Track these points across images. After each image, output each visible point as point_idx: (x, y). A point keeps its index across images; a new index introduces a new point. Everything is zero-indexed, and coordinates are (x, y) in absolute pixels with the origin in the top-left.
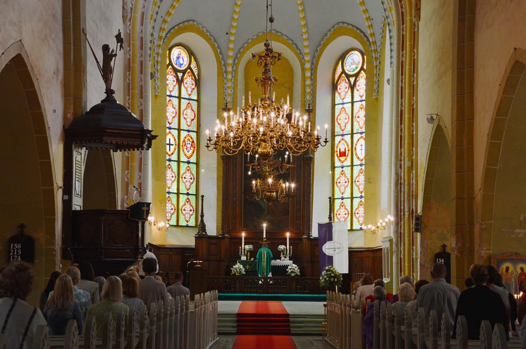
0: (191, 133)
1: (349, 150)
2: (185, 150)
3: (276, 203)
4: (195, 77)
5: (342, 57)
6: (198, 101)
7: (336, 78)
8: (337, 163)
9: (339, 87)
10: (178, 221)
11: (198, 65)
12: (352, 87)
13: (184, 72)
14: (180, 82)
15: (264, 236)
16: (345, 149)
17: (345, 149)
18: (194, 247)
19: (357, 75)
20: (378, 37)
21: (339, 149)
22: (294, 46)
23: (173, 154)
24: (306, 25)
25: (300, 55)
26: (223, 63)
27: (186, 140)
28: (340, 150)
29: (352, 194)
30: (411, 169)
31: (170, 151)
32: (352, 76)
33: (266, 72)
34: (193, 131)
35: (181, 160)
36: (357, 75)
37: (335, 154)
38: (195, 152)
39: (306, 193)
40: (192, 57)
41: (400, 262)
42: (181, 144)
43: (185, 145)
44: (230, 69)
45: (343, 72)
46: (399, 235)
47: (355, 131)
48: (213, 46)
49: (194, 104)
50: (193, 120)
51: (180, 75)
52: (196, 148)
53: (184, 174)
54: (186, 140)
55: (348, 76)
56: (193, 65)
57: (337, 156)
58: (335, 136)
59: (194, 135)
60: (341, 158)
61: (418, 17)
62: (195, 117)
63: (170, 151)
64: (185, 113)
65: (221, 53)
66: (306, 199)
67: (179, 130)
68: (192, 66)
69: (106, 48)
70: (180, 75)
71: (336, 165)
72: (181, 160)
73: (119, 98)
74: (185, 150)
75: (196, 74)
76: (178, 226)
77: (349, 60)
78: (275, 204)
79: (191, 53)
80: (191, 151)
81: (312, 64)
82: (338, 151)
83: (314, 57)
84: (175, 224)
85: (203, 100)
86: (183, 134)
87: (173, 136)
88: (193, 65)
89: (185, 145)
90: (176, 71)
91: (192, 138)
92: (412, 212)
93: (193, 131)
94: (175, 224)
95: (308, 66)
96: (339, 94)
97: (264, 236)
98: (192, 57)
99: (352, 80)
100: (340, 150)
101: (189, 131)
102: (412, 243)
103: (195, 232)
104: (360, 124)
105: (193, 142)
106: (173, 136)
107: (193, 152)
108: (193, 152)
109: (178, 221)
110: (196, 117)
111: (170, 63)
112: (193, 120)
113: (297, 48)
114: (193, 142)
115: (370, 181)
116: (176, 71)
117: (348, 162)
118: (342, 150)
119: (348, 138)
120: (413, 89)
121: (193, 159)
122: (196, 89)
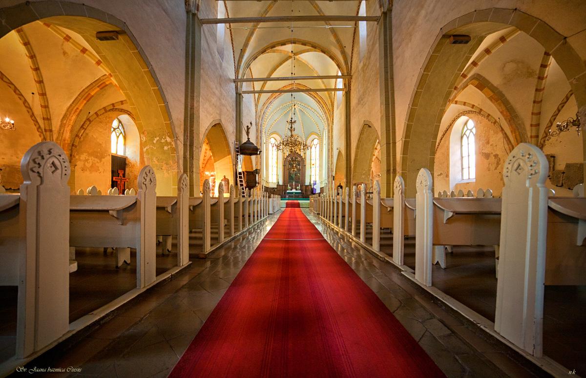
20: (321, 133)
30: (331, 164)
41: (329, 188)
46: (329, 182)
61: (333, 124)
69: (248, 126)
73: (251, 141)
92: (332, 176)
102: (332, 183)
104: (318, 157)
120: (332, 143)
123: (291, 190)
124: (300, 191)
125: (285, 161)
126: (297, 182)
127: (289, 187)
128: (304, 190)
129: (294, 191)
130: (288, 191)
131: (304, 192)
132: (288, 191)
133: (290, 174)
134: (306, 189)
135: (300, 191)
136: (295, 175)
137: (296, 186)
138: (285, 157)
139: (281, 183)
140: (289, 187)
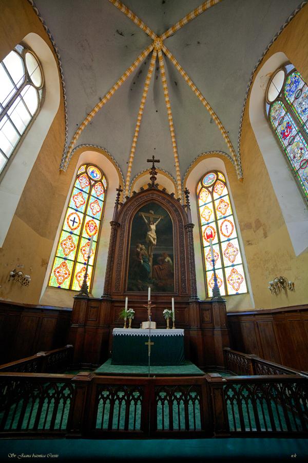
0: (94, 220)
1: (215, 232)
2: (88, 230)
3: (161, 266)
4: (104, 188)
5: (201, 180)
6: (104, 202)
7: (198, 191)
8: (205, 243)
9: (200, 196)
10: (71, 285)
11: (107, 182)
12: (212, 193)
13: (96, 182)
14: (92, 186)
15: (149, 299)
16: (212, 232)
17: (212, 232)
18: (71, 310)
19: (213, 185)
21: (206, 233)
22: (170, 175)
23: (75, 229)
24: (178, 157)
25: (174, 180)
26: (123, 180)
27: (90, 223)
28: (207, 234)
29: (223, 264)
31: (73, 226)
32: (210, 187)
33: (153, 178)
34: (97, 219)
35: (83, 236)
36: (213, 185)
37: (203, 238)
38: (97, 234)
39: (189, 257)
40: (104, 177)
42: (85, 225)
43: (89, 226)
44: (128, 183)
45: (203, 187)
47: (218, 218)
48: (118, 170)
49: (101, 204)
50: (98, 212)
51: (93, 183)
52: (98, 231)
53: (84, 247)
54: (90, 223)
55: (207, 188)
56: (104, 181)
57: (205, 239)
58: (201, 226)
59: (98, 223)
60: (209, 240)
62: (100, 210)
63: (73, 226)
64: (92, 205)
65: (123, 175)
66: (190, 262)
67: (85, 214)
68: (102, 181)
70: (93, 183)
71: (205, 246)
72: (83, 236)
74: (88, 230)
75: (105, 186)
76: (70, 290)
77: (206, 179)
78: (160, 268)
79: (103, 174)
80: (93, 232)
81: (182, 183)
82: (206, 235)
83: (183, 179)
84: (67, 288)
85: (108, 201)
86: (88, 219)
87: (78, 216)
88: (104, 181)
89: (89, 226)
90: (90, 179)
91: (95, 223)
93: (97, 219)
94: (67, 288)
95: (179, 182)
96: (202, 200)
97: (149, 299)
98: (104, 177)
99: (210, 189)
100: (207, 234)
101: (93, 218)
103: (78, 293)
105: (96, 226)
106: (78, 216)
107: (95, 233)
108: (95, 233)
109: (71, 285)
110: (101, 211)
111: (86, 172)
112: (98, 212)
113: (172, 176)
114: (96, 226)
115: (250, 242)
116: (90, 179)
117: (216, 240)
118: (209, 233)
119: (214, 225)
121: (95, 238)
122: (104, 194)
123: (136, 324)
124: (180, 332)
125: (121, 209)
126: (164, 290)
127: (128, 311)
128: (194, 326)
129: (148, 328)
130: (117, 331)
131: (194, 333)
132: (117, 331)
133: (134, 257)
134: (202, 320)
135: (180, 332)
136: (155, 262)
137: (160, 304)
138: (123, 200)
139: (98, 292)
140: (128, 311)
